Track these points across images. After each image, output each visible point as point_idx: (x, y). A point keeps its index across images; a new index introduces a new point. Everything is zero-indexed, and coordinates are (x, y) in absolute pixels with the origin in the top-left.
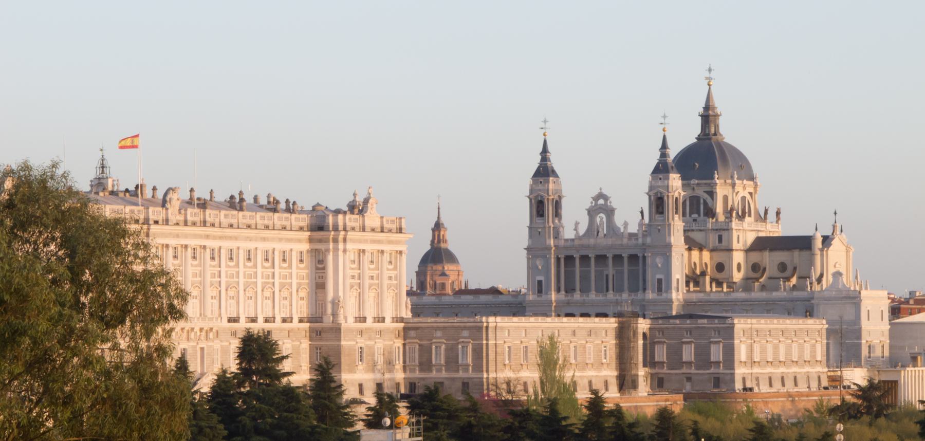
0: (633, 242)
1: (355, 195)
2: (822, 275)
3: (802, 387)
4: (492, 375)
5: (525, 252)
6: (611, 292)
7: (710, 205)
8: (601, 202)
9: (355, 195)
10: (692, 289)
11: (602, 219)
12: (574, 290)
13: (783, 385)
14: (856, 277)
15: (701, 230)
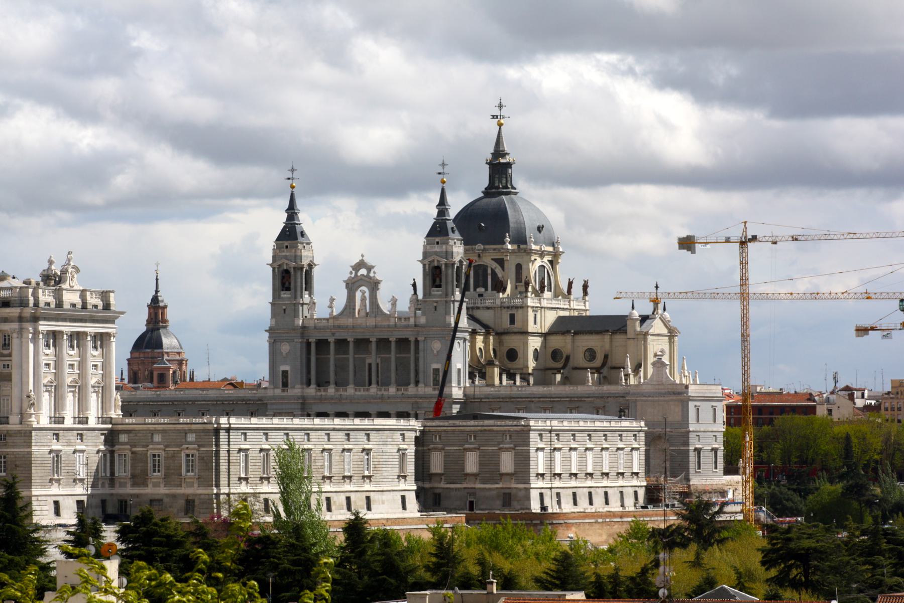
0: (404, 323)
1: (51, 262)
2: (639, 366)
3: (615, 506)
4: (224, 490)
5: (267, 334)
6: (374, 386)
7: (500, 275)
8: (363, 271)
9: (51, 262)
10: (477, 383)
11: (364, 293)
12: (328, 383)
13: (591, 503)
14: (683, 368)
15: (488, 308)
